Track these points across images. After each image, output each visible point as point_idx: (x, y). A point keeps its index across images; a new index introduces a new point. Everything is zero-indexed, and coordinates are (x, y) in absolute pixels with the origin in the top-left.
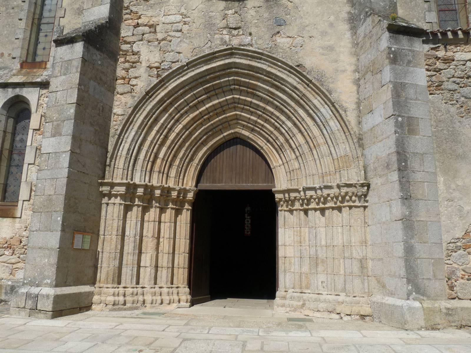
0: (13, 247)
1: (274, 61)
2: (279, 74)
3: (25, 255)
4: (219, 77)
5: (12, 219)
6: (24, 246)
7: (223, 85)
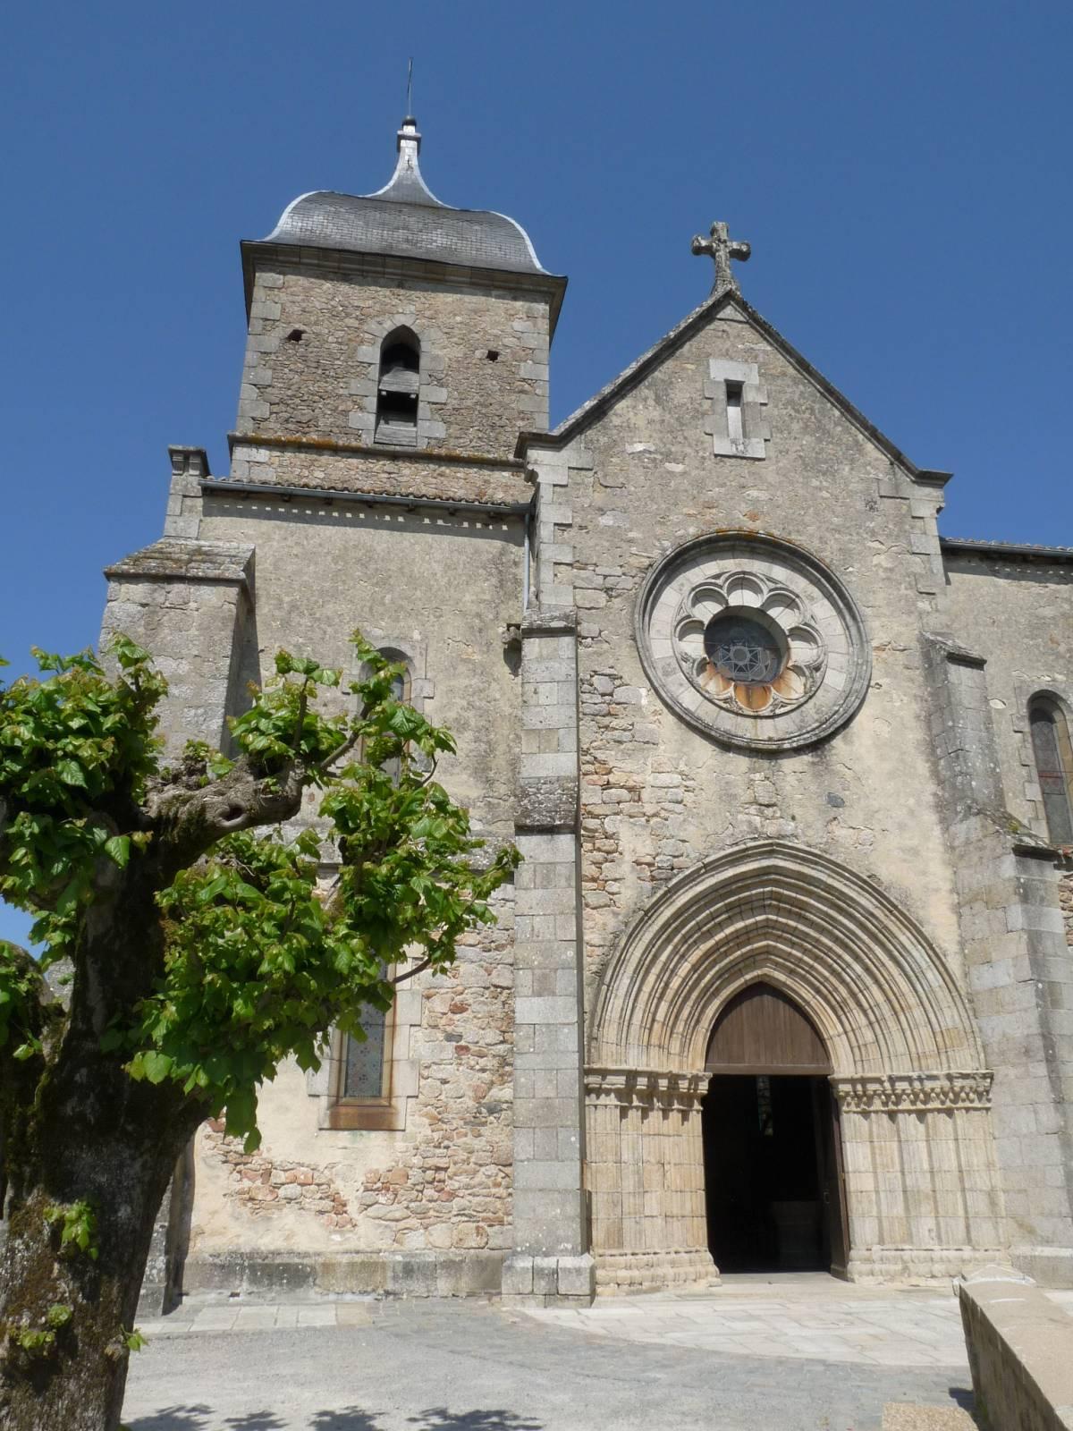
0: (395, 1190)
1: (838, 869)
2: (846, 890)
3: (418, 1203)
4: (748, 888)
5: (387, 1133)
6: (415, 1185)
7: (754, 898)
